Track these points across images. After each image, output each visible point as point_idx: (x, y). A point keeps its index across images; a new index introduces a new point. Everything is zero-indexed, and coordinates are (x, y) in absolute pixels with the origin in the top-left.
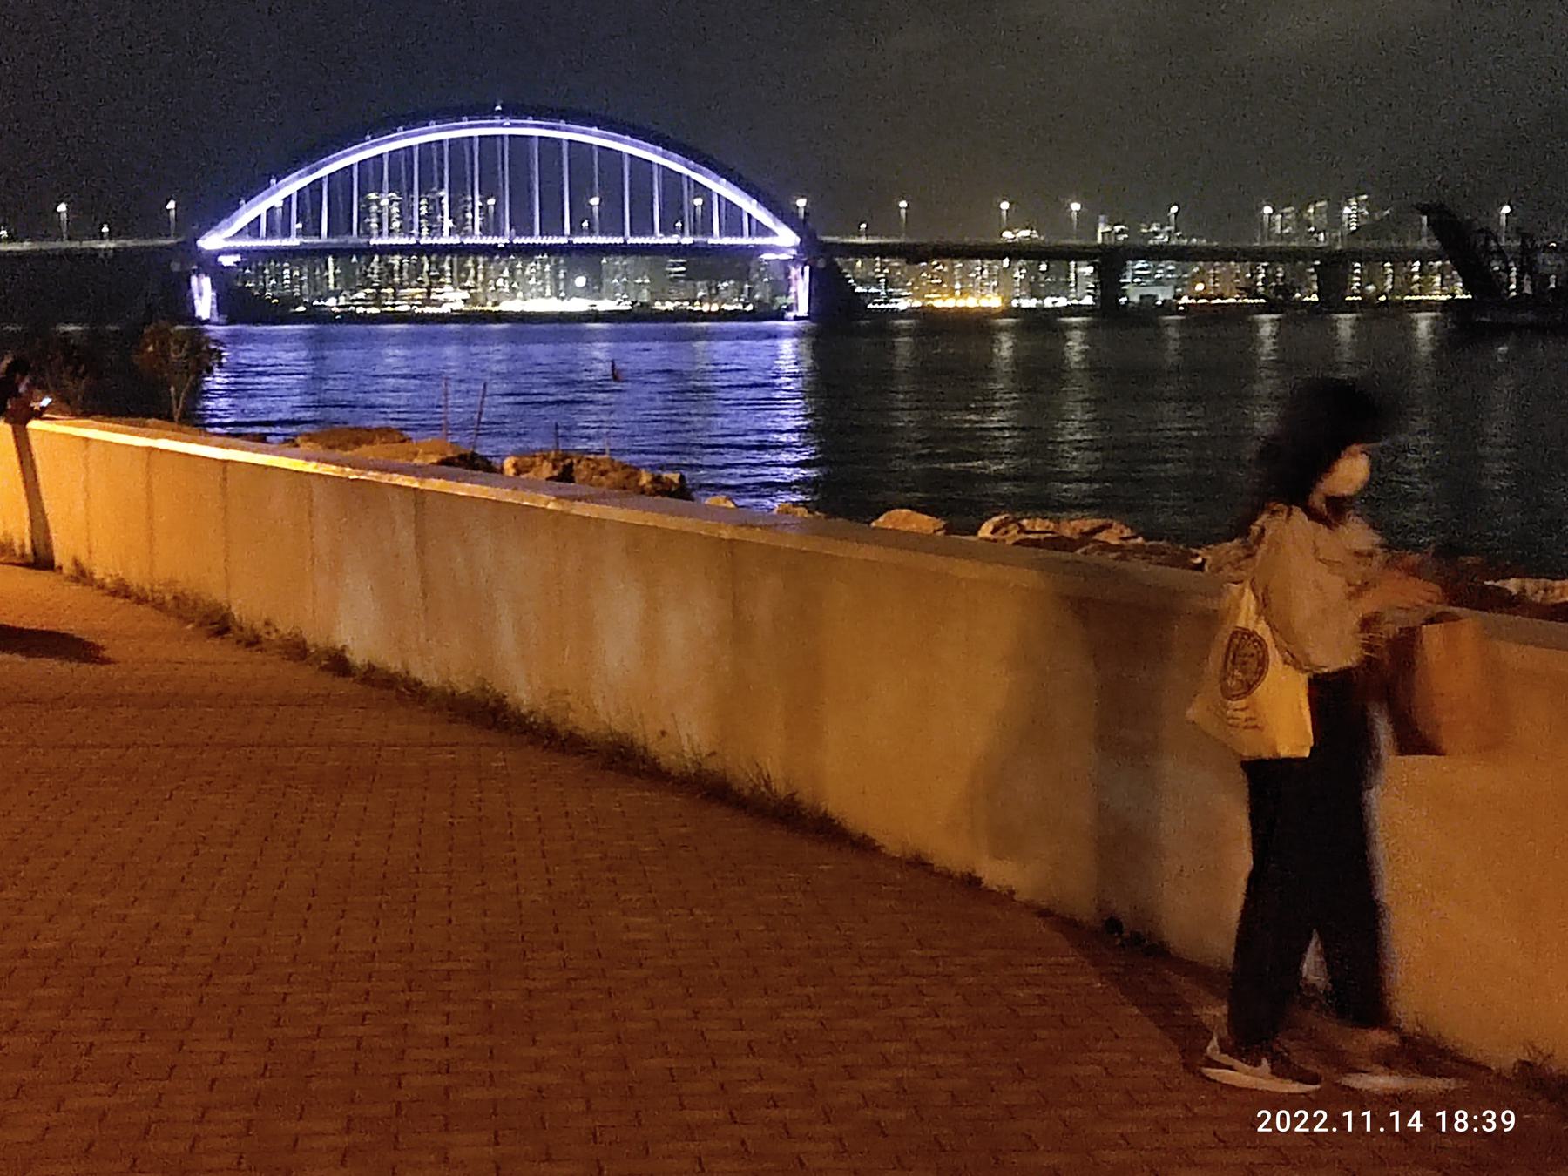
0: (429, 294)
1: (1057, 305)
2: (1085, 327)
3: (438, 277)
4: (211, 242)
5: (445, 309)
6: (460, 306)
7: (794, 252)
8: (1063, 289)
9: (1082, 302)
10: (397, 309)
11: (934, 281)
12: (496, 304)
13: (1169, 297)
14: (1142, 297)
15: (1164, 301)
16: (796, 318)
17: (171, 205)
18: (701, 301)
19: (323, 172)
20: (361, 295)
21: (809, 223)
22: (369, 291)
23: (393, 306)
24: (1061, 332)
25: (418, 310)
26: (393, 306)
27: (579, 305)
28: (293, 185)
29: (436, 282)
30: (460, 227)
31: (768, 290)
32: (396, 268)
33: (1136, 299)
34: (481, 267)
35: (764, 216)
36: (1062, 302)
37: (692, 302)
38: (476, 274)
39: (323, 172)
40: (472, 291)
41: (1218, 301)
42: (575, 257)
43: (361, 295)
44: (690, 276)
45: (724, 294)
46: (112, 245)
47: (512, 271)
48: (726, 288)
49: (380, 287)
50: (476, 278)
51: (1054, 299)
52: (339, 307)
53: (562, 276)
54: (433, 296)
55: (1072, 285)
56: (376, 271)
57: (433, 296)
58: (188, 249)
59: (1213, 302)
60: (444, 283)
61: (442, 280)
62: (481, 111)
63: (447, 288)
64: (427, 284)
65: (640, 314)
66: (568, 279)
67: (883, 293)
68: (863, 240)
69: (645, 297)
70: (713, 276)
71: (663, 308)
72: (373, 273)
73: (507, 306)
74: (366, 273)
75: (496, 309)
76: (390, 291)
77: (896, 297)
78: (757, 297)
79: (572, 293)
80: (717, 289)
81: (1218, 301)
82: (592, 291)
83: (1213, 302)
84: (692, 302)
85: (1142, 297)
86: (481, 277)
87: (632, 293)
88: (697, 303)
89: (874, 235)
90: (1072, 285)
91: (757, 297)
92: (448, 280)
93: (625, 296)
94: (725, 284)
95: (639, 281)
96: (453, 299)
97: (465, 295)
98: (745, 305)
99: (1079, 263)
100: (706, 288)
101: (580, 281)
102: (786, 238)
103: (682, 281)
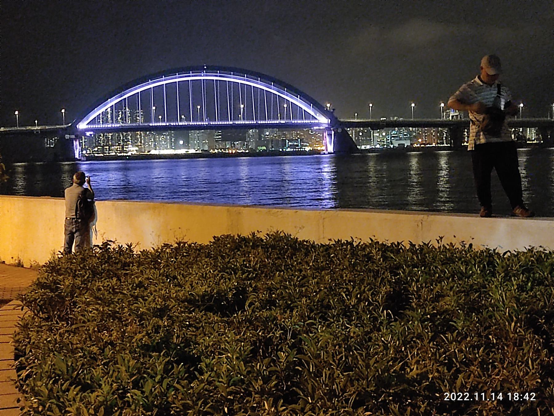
0: (123, 148)
1: (367, 148)
2: (448, 155)
3: (126, 142)
4: (82, 126)
5: (129, 154)
6: (135, 152)
7: (327, 126)
8: (369, 142)
9: (376, 147)
10: (110, 154)
11: (317, 140)
12: (149, 152)
13: (409, 144)
14: (399, 144)
15: (407, 146)
16: (329, 153)
17: (63, 111)
18: (228, 149)
19: (126, 96)
20: (96, 149)
21: (334, 114)
22: (99, 147)
23: (109, 153)
24: (437, 157)
25: (119, 155)
26: (109, 153)
27: (182, 151)
28: (113, 101)
29: (126, 142)
30: (134, 120)
31: (254, 144)
32: (110, 139)
33: (397, 145)
34: (143, 137)
35: (311, 111)
36: (368, 147)
37: (225, 149)
38: (141, 140)
39: (126, 96)
40: (140, 147)
41: (428, 145)
42: (178, 132)
43: (96, 149)
44: (224, 139)
45: (237, 146)
46: (39, 128)
47: (155, 139)
48: (237, 144)
49: (104, 146)
50: (141, 142)
51: (365, 146)
52: (87, 154)
53: (173, 140)
54: (125, 149)
55: (372, 140)
56: (102, 140)
57: (125, 149)
58: (73, 130)
59: (427, 146)
60: (129, 144)
61: (128, 143)
62: (198, 69)
63: (130, 146)
64: (122, 144)
65: (205, 155)
66: (176, 141)
67: (299, 145)
68: (356, 120)
69: (206, 148)
70: (233, 140)
71: (214, 152)
72: (101, 141)
73: (153, 152)
74: (98, 141)
75: (149, 153)
76: (107, 147)
77: (305, 146)
78: (250, 147)
79: (177, 147)
80: (234, 144)
81: (428, 145)
82: (187, 144)
83: (427, 146)
84: (225, 149)
85: (399, 144)
86: (143, 141)
87: (201, 146)
88: (227, 150)
89: (361, 118)
90: (372, 140)
91: (250, 147)
92: (130, 143)
93: (199, 148)
94: (237, 143)
95: (204, 142)
96: (132, 150)
97: (137, 149)
98: (245, 150)
99: (374, 131)
100: (230, 144)
101: (181, 142)
102: (323, 120)
103: (220, 142)
